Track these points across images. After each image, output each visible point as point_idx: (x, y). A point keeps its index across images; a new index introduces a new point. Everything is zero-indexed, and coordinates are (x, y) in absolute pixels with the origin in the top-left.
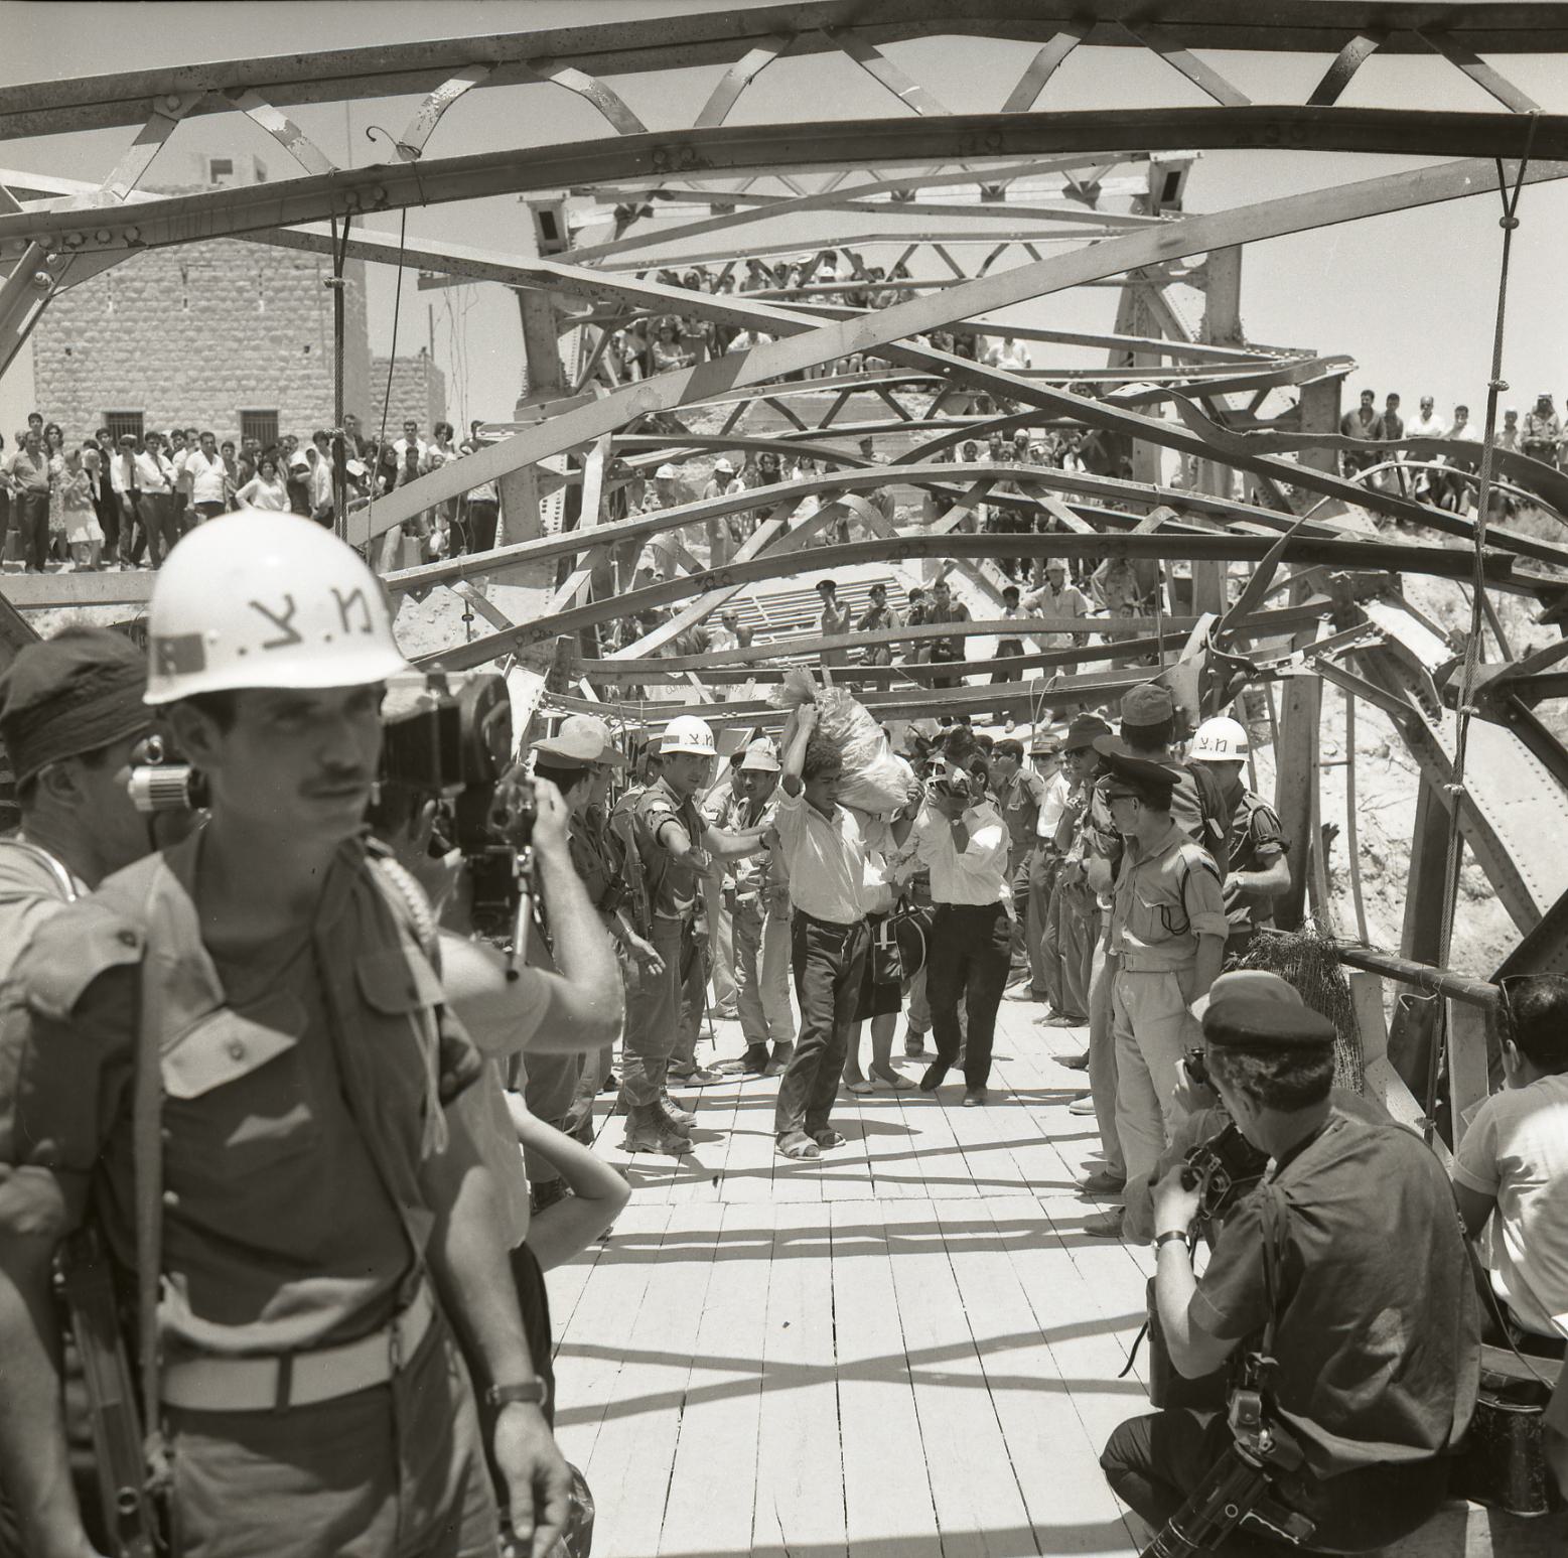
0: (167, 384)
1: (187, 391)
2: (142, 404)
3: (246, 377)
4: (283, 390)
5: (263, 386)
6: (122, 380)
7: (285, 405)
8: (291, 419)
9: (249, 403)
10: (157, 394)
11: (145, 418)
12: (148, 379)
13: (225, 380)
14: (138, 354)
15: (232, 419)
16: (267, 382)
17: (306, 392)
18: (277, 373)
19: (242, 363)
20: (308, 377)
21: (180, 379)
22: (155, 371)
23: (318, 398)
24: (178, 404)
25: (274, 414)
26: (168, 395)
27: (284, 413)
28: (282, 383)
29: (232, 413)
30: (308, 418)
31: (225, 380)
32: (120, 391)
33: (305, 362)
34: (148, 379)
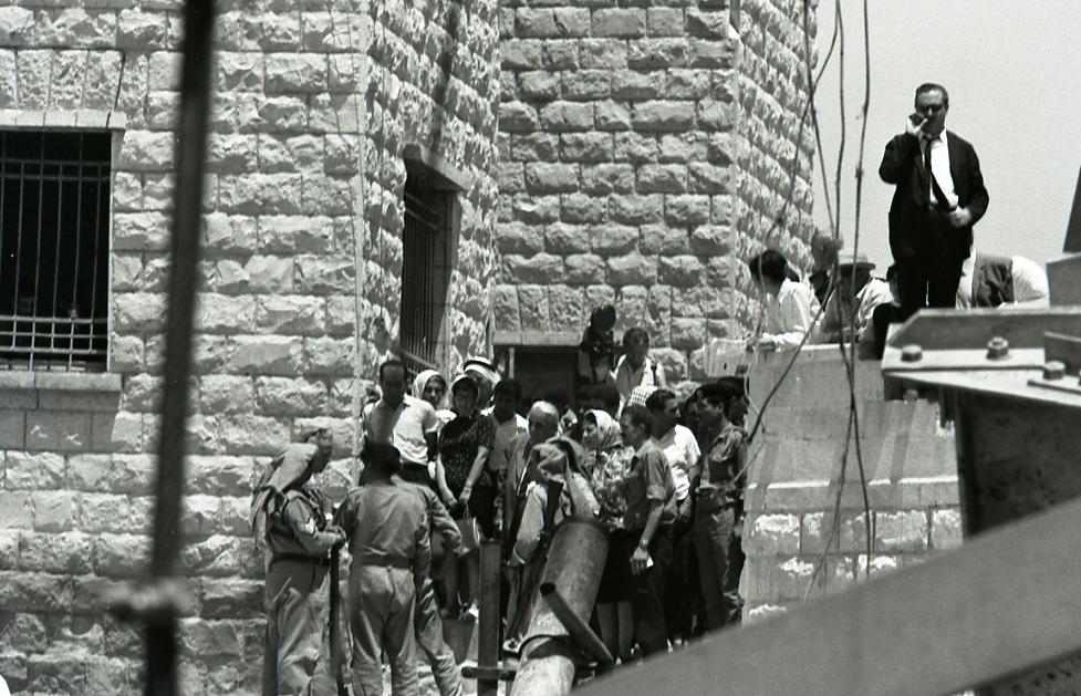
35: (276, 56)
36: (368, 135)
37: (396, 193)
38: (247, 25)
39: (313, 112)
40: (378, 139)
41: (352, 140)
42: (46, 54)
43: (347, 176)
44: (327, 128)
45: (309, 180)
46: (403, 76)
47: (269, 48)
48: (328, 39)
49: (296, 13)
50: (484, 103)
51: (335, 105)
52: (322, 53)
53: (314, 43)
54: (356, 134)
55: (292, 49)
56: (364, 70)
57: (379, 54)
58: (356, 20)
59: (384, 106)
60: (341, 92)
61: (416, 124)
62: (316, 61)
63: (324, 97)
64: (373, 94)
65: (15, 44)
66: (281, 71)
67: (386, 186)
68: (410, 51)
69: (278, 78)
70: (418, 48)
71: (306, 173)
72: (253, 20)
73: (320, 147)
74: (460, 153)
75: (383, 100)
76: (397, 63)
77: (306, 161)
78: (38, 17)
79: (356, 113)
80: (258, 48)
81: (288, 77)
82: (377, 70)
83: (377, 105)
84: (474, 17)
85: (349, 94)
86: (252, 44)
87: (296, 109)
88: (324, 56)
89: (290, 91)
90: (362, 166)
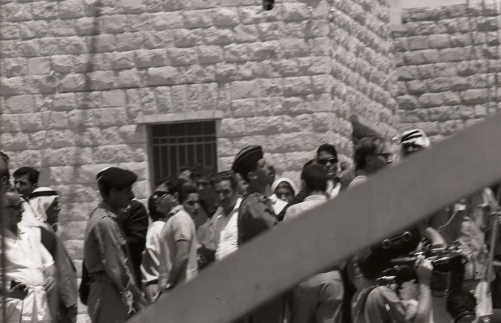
1: (52, 92)
3: (157, 61)
9: (164, 110)
15: (134, 145)
19: (150, 34)
20: (271, 53)
21: (38, 70)
24: (33, 118)
27: (228, 123)
29: (131, 129)
31: (117, 68)
33: (265, 26)
35: (288, 78)
36: (333, 112)
37: (348, 137)
38: (274, 66)
39: (307, 103)
40: (339, 114)
41: (325, 115)
42: (183, 87)
43: (324, 131)
44: (314, 110)
45: (307, 135)
46: (348, 83)
47: (284, 75)
48: (312, 69)
49: (295, 58)
50: (387, 94)
51: (316, 99)
52: (309, 75)
53: (305, 71)
54: (326, 111)
55: (294, 75)
56: (329, 82)
57: (335, 74)
58: (324, 59)
59: (339, 98)
60: (318, 93)
61: (355, 105)
62: (306, 79)
63: (310, 96)
64: (334, 93)
65: (170, 83)
66: (290, 86)
67: (343, 134)
68: (349, 71)
69: (290, 89)
70: (354, 70)
71: (305, 132)
72: (276, 63)
73: (310, 119)
74: (377, 117)
75: (338, 95)
76: (344, 77)
77: (305, 126)
78: (180, 71)
79: (328, 102)
80: (279, 76)
81: (294, 88)
82: (335, 82)
83: (336, 98)
84: (379, 55)
85: (323, 93)
86: (276, 74)
87: (298, 103)
88: (309, 77)
89: (296, 95)
90: (330, 126)
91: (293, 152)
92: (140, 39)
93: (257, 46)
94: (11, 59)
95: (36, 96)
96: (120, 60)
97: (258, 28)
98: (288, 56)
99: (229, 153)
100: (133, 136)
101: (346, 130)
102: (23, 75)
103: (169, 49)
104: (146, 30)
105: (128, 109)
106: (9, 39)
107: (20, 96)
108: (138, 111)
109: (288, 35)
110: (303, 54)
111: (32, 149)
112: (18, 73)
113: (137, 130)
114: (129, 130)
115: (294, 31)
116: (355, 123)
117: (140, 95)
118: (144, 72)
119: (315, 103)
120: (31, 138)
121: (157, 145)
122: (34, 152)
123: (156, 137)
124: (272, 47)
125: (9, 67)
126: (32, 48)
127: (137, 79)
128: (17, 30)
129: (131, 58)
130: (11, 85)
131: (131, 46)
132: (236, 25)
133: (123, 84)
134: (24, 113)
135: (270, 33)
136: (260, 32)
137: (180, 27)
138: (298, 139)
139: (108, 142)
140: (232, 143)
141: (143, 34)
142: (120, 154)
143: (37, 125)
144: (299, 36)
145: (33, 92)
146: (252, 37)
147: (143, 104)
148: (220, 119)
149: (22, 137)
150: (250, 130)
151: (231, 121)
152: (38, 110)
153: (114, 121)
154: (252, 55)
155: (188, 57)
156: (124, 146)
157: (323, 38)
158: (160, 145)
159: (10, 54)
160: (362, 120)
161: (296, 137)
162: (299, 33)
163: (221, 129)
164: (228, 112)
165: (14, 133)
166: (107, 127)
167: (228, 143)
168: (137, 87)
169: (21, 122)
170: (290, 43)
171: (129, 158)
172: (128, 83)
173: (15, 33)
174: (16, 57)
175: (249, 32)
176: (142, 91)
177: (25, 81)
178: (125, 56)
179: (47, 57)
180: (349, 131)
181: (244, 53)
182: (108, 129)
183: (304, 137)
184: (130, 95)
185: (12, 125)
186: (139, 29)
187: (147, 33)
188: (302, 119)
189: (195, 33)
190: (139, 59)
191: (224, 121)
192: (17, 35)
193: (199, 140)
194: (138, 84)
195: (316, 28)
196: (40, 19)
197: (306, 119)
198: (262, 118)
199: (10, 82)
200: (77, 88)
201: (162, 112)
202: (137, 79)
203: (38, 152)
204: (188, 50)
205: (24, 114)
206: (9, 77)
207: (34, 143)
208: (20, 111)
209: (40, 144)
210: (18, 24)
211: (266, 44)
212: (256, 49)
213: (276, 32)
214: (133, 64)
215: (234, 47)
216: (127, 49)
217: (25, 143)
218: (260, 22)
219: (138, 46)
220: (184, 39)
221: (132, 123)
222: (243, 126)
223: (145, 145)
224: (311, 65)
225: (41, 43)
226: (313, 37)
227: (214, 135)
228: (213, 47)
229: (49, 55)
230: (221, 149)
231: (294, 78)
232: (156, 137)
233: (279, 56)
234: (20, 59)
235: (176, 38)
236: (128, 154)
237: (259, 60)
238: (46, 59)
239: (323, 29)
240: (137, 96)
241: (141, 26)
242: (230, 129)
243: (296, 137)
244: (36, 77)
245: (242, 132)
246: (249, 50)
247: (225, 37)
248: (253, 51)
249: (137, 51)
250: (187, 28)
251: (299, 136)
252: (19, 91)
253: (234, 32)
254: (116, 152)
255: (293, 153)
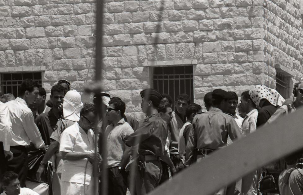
0: (70, 40)
2: (38, 64)
4: (197, 42)
5: (176, 37)
6: (20, 36)
7: (203, 60)
8: (207, 75)
10: (59, 52)
11: (44, 78)
12: (48, 35)
13: (132, 33)
14: (37, 8)
16: (182, 33)
17: (226, 43)
18: (191, 23)
20: (228, 26)
22: (56, 25)
23: (239, 50)
25: (189, 70)
26: (68, 52)
27: (200, 67)
28: (198, 34)
29: (141, 69)
30: (227, 72)
31: (132, 33)
32: (17, 49)
33: (224, 9)
34: (48, 35)
35: (238, 41)
36: (264, 62)
38: (229, 33)
39: (249, 56)
40: (268, 63)
41: (260, 63)
42: (173, 45)
43: (259, 73)
45: (249, 75)
46: (274, 45)
47: (235, 39)
48: (252, 36)
49: (243, 29)
50: (298, 52)
51: (255, 54)
52: (250, 39)
53: (248, 37)
54: (261, 62)
55: (242, 39)
56: (263, 44)
57: (266, 39)
59: (269, 53)
60: (256, 50)
61: (278, 58)
62: (249, 42)
63: (251, 52)
64: (266, 51)
67: (271, 76)
68: (275, 38)
69: (239, 47)
70: (278, 37)
71: (248, 73)
72: (231, 32)
74: (292, 66)
75: (268, 52)
76: (272, 41)
77: (248, 70)
78: (171, 35)
79: (262, 56)
80: (233, 39)
81: (241, 47)
82: (266, 43)
83: (267, 53)
84: (294, 28)
85: (259, 50)
86: (231, 38)
87: (244, 56)
88: (251, 40)
90: (263, 71)
91: (239, 85)
92: (148, 15)
93: (219, 21)
94: (68, 26)
95: (82, 48)
96: (134, 28)
97: (220, 10)
98: (238, 28)
99: (201, 85)
100: (141, 74)
101: (273, 73)
102: (75, 36)
103: (165, 22)
104: (151, 10)
105: (138, 57)
106: (67, 14)
107: (73, 48)
108: (146, 58)
109: (238, 15)
110: (247, 27)
111: (79, 80)
112: (72, 35)
113: (144, 70)
114: (139, 70)
115: (242, 12)
116: (278, 69)
117: (146, 49)
118: (149, 35)
119: (255, 56)
120: (79, 74)
121: (156, 79)
122: (81, 82)
123: (156, 75)
124: (229, 22)
125: (66, 31)
126: (81, 20)
127: (144, 39)
128: (72, 9)
129: (141, 27)
130: (68, 42)
131: (142, 20)
132: (207, 8)
133: (136, 42)
134: (75, 58)
135: (228, 13)
136: (222, 12)
137: (172, 9)
138: (243, 78)
139: (126, 77)
140: (203, 79)
141: (150, 12)
142: (133, 85)
143: (83, 65)
144: (245, 16)
145: (81, 46)
146: (217, 16)
147: (148, 55)
148: (196, 65)
149: (73, 73)
150: (213, 72)
151: (202, 66)
152: (84, 57)
153: (130, 65)
154: (216, 26)
155: (177, 27)
156: (136, 79)
157: (260, 17)
158: (158, 79)
159: (67, 23)
160: (282, 67)
161: (242, 77)
162: (246, 14)
163: (196, 70)
164: (201, 61)
165: (68, 70)
166: (126, 68)
167: (200, 79)
168: (145, 45)
169: (72, 64)
170: (240, 20)
171: (139, 87)
172: (139, 41)
173: (71, 10)
174: (71, 25)
175: (215, 12)
176: (147, 47)
177: (76, 39)
178: (138, 26)
179: (89, 26)
180: (274, 74)
181: (211, 25)
182: (126, 69)
183: (246, 77)
184: (140, 49)
185: (67, 66)
186: (146, 9)
187: (152, 12)
188: (247, 66)
189: (181, 13)
190: (146, 28)
191: (198, 66)
192: (72, 12)
193: (182, 77)
194: (146, 43)
195: (256, 11)
196: (86, 3)
197: (249, 66)
198: (222, 65)
199: (67, 40)
200: (108, 44)
201: (159, 60)
202: (144, 39)
203: (83, 82)
204: (177, 23)
205: (75, 59)
206: (66, 37)
207: (81, 77)
208: (73, 57)
209: (84, 77)
210: (72, 5)
211: (225, 20)
212: (219, 23)
213: (231, 13)
214: (142, 31)
215: (205, 21)
216: (139, 21)
217: (75, 76)
218: (222, 7)
219: (146, 20)
220: (175, 16)
221: (141, 66)
222: (209, 69)
223: (148, 79)
224: (252, 34)
225: (86, 17)
226: (254, 17)
227: (192, 74)
228: (193, 21)
229: (91, 24)
230: (196, 83)
231: (241, 41)
232: (156, 75)
233: (233, 27)
234: (73, 26)
235: (169, 15)
236: (138, 84)
237: (220, 30)
238: (90, 26)
239: (260, 12)
240: (144, 50)
241: (148, 8)
242: (201, 71)
243: (242, 77)
244: (83, 37)
245: (209, 73)
246: (214, 23)
247: (200, 15)
248: (217, 24)
249: (145, 23)
250: (176, 10)
251: (244, 76)
252: (72, 45)
253: (205, 12)
254: (130, 83)
255: (239, 86)
